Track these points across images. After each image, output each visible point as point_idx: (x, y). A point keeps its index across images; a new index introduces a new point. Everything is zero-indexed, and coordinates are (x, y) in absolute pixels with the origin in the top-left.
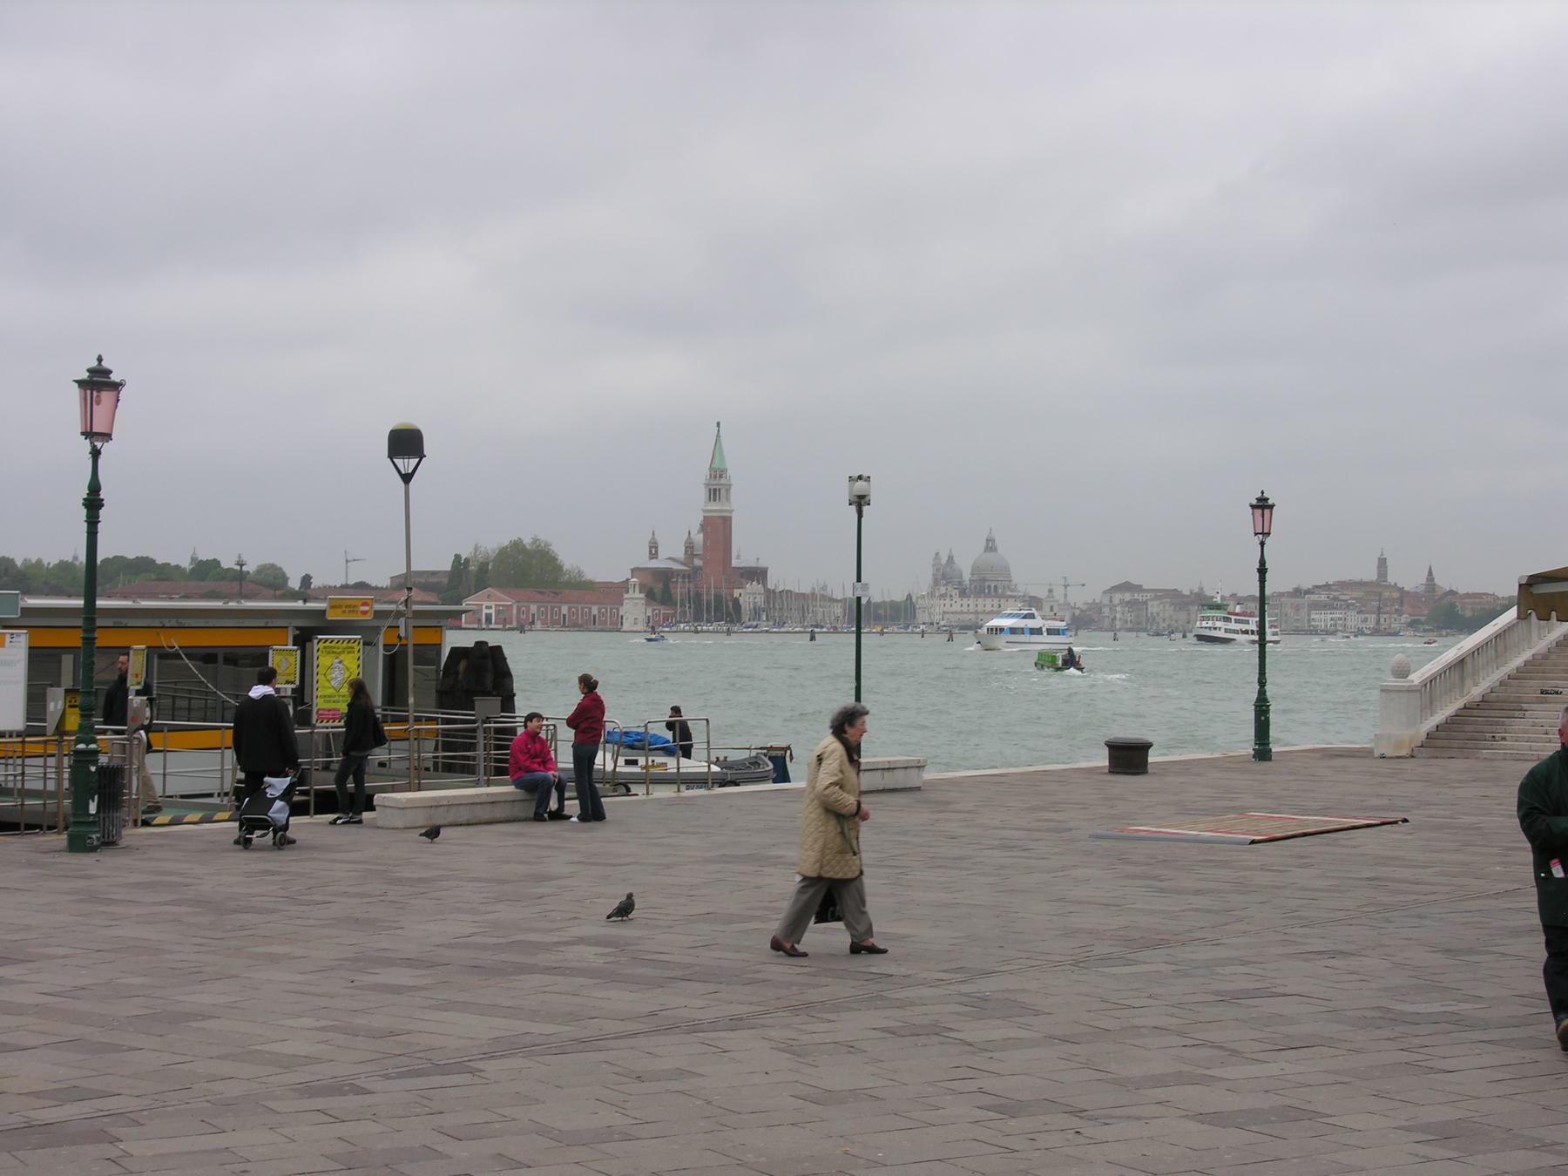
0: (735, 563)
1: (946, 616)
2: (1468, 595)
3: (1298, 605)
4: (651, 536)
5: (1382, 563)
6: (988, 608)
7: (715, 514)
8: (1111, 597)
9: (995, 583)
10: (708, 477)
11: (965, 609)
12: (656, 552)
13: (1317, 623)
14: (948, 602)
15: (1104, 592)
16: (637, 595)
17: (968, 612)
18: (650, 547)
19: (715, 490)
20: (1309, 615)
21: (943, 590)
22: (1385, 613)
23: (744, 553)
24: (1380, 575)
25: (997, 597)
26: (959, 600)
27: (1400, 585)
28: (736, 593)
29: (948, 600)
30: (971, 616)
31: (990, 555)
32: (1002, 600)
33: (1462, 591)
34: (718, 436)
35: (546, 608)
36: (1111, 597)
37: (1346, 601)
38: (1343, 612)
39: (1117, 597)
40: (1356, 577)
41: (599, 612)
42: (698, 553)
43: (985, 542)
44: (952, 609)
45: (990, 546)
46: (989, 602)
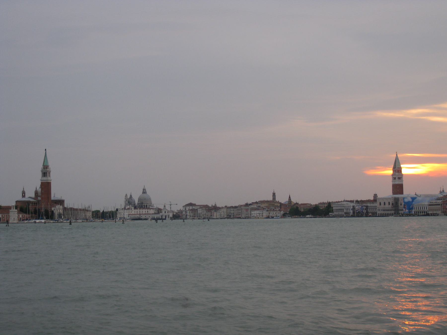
0: (52, 198)
1: (130, 216)
2: (302, 204)
3: (247, 209)
4: (23, 190)
5: (274, 194)
6: (144, 213)
7: (45, 181)
8: (185, 208)
9: (146, 204)
10: (42, 169)
11: (136, 213)
12: (25, 195)
13: (253, 215)
14: (130, 211)
15: (183, 207)
16: (15, 210)
17: (137, 214)
18: (23, 194)
19: (45, 173)
20: (251, 212)
21: (128, 207)
22: (276, 211)
23: (55, 194)
24: (273, 199)
25: (147, 209)
26: (134, 211)
27: (280, 202)
28: (53, 209)
29: (130, 210)
30: (138, 216)
31: (144, 195)
32: (149, 210)
33: (300, 203)
34: (46, 154)
35: (5, 216)
36: (185, 208)
37: (263, 207)
38: (262, 211)
39: (188, 208)
40: (266, 199)
41: (22, 217)
42: (39, 195)
43: (143, 190)
44: (132, 213)
45: (144, 192)
46: (144, 210)
